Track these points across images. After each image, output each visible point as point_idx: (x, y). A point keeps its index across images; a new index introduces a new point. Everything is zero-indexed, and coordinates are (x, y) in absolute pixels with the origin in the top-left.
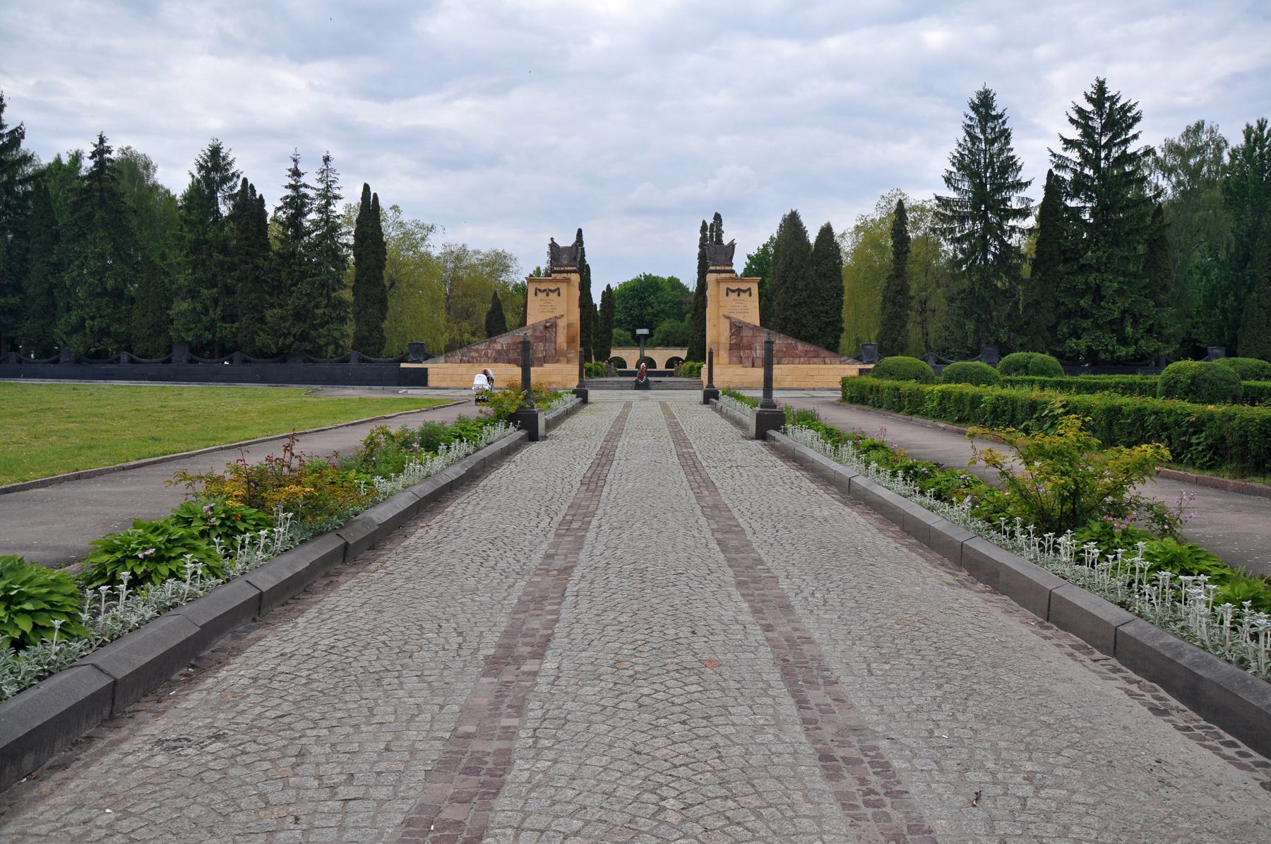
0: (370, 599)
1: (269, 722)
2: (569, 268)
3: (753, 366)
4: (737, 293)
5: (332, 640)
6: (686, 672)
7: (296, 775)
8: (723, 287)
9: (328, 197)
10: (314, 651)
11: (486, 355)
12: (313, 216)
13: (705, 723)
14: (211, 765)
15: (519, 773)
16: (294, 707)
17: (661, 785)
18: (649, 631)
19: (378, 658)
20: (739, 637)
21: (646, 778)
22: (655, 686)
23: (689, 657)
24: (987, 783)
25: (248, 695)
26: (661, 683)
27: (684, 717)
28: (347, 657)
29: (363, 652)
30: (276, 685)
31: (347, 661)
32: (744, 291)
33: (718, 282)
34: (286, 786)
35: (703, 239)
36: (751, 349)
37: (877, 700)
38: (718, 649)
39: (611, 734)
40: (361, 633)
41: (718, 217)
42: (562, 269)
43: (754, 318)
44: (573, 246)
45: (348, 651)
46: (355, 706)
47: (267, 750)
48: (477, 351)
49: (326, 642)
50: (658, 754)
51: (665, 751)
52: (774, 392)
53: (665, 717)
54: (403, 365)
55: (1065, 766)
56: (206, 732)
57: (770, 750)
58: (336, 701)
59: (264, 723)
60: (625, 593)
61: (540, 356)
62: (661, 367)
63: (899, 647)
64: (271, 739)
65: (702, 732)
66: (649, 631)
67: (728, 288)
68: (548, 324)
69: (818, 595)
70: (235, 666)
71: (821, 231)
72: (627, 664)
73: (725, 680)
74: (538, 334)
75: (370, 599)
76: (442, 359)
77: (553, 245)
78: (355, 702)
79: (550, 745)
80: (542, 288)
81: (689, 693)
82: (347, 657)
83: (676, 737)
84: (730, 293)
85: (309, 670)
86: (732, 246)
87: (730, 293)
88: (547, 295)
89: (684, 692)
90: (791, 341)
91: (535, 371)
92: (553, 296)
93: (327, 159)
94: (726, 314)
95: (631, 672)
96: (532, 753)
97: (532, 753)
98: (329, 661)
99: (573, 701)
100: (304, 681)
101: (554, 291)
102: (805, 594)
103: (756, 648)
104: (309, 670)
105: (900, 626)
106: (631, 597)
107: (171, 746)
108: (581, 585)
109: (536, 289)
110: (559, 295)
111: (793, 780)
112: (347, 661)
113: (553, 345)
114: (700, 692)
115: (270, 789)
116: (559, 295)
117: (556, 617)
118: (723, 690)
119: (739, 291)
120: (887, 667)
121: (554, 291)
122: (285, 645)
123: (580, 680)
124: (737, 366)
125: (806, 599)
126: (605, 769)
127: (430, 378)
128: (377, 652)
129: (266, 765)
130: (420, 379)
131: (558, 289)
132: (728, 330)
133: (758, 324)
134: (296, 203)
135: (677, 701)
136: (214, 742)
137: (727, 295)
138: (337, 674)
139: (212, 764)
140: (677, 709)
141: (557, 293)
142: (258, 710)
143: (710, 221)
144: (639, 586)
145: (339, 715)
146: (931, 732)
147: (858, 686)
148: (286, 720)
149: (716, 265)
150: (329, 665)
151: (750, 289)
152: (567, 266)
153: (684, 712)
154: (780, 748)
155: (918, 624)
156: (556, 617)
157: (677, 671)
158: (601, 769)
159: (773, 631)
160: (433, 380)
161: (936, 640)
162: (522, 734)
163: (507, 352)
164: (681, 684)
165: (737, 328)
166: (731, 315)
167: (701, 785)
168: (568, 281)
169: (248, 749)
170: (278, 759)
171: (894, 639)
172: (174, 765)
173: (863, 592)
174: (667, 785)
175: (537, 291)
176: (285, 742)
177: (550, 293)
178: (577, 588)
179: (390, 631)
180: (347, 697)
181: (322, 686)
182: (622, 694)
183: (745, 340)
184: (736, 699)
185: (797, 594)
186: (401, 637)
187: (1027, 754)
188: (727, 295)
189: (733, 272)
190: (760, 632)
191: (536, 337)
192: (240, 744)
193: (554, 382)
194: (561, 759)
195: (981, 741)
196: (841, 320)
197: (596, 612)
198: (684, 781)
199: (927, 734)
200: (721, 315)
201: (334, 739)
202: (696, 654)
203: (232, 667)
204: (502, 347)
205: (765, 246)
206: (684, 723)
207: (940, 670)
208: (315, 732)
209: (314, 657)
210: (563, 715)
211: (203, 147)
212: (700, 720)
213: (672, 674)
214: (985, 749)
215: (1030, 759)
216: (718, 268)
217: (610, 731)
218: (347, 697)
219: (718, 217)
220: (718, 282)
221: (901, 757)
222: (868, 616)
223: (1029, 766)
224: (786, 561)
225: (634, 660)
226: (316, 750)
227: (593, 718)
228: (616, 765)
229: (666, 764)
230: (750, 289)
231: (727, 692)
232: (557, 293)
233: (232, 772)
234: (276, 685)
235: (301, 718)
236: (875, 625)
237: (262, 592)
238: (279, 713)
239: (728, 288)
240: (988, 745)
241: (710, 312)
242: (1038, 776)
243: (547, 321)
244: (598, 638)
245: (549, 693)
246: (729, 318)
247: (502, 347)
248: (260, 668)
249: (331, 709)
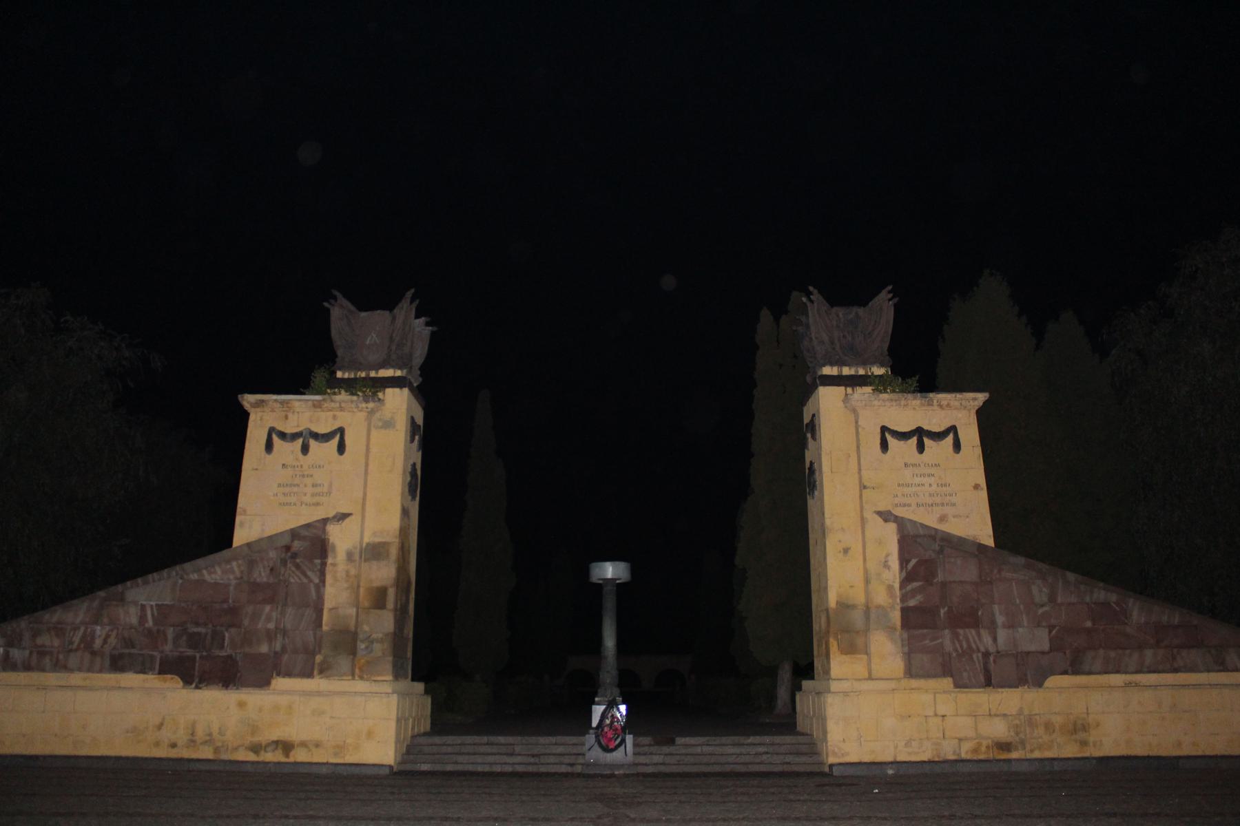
3: (988, 683)
4: (914, 441)
11: (87, 643)
32: (938, 436)
36: (976, 624)
48: (59, 630)
61: (264, 649)
67: (884, 429)
80: (289, 429)
88: (305, 449)
90: (1101, 594)
92: (323, 452)
101: (326, 438)
110: (341, 448)
113: (309, 613)
116: (341, 448)
119: (920, 435)
124: (932, 683)
133: (990, 542)
137: (884, 446)
149: (841, 363)
163: (154, 637)
166: (900, 512)
177: (313, 443)
188: (884, 446)
191: (255, 587)
193: (303, 744)
200: (869, 515)
204: (143, 618)
230: (953, 429)
239: (884, 429)
243: (294, 534)
247: (143, 618)
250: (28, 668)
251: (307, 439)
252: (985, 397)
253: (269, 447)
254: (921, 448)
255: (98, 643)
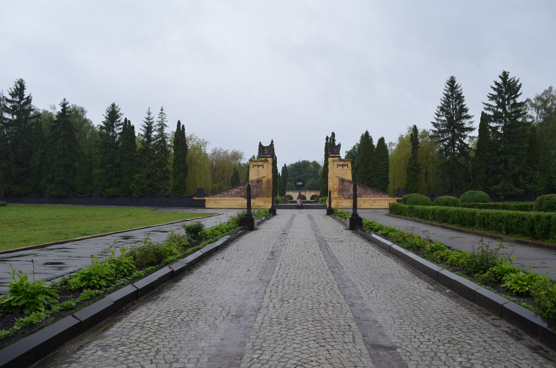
0: (183, 293)
1: (144, 339)
2: (268, 156)
4: (341, 166)
5: (168, 309)
6: (316, 322)
7: (155, 359)
8: (336, 164)
9: (162, 126)
10: (161, 313)
12: (155, 133)
13: (323, 341)
14: (121, 355)
15: (246, 359)
16: (153, 334)
17: (305, 363)
18: (301, 306)
19: (188, 316)
20: (339, 308)
21: (299, 360)
22: (303, 327)
23: (318, 316)
24: (442, 365)
25: (134, 329)
26: (306, 326)
27: (315, 338)
28: (175, 315)
29: (181, 313)
30: (145, 325)
31: (174, 316)
32: (345, 165)
33: (334, 161)
34: (152, 363)
35: (327, 144)
36: (348, 191)
37: (397, 334)
38: (330, 313)
39: (285, 344)
40: (180, 306)
41: (333, 134)
42: (265, 156)
43: (349, 176)
44: (269, 146)
45: (175, 313)
46: (179, 334)
47: (143, 350)
49: (166, 309)
50: (304, 352)
51: (306, 351)
52: (358, 210)
53: (307, 338)
54: (194, 198)
55: (476, 359)
56: (118, 343)
57: (350, 351)
58: (171, 332)
59: (141, 340)
60: (291, 291)
62: (308, 198)
63: (407, 313)
64: (144, 345)
65: (322, 344)
66: (301, 306)
68: (258, 180)
69: (374, 292)
70: (128, 318)
71: (379, 140)
72: (291, 318)
73: (333, 325)
74: (254, 184)
75: (183, 293)
76: (212, 196)
77: (260, 145)
78: (179, 332)
79: (259, 348)
81: (317, 329)
82: (175, 315)
83: (311, 346)
84: (338, 166)
85: (159, 320)
86: (339, 145)
87: (338, 166)
88: (258, 167)
89: (315, 329)
91: (252, 201)
92: (261, 168)
93: (162, 110)
94: (337, 175)
95: (293, 321)
96: (252, 351)
97: (252, 351)
98: (167, 317)
99: (269, 332)
100: (157, 324)
102: (368, 292)
103: (346, 313)
104: (159, 320)
105: (408, 305)
106: (293, 293)
107: (104, 349)
108: (272, 288)
109: (253, 165)
110: (263, 167)
111: (360, 363)
112: (174, 316)
114: (322, 329)
115: (145, 364)
116: (263, 167)
117: (262, 300)
118: (332, 329)
120: (402, 321)
121: (261, 166)
122: (149, 311)
123: (272, 324)
125: (368, 294)
126: (282, 357)
127: (206, 204)
128: (187, 313)
129: (143, 355)
130: (201, 205)
131: (263, 165)
132: (338, 182)
133: (351, 180)
134: (149, 129)
135: (312, 332)
136: (121, 346)
137: (337, 167)
138: (171, 322)
139: (121, 354)
140: (313, 335)
141: (262, 167)
142: (138, 335)
143: (330, 136)
144: (297, 288)
145: (172, 337)
146: (419, 346)
147: (389, 328)
148: (150, 338)
149: (333, 154)
150: (167, 318)
151: (347, 164)
152: (267, 155)
153: (314, 337)
154: (355, 351)
155: (416, 304)
156: (262, 300)
157: (313, 321)
158: (280, 357)
159: (354, 306)
160: (207, 205)
161: (423, 311)
162: (248, 344)
164: (314, 326)
165: (342, 181)
166: (340, 176)
167: (321, 364)
168: (267, 161)
169: (135, 349)
170: (148, 353)
171: (405, 311)
172: (106, 355)
173: (393, 291)
174: (307, 363)
175: (254, 166)
176: (150, 347)
178: (271, 289)
179: (192, 305)
180: (175, 330)
181: (164, 326)
182: (290, 329)
183: (346, 187)
184: (337, 332)
185: (365, 292)
186: (197, 308)
187: (459, 355)
188: (337, 167)
189: (340, 157)
190: (348, 307)
192: (133, 347)
194: (263, 354)
195: (440, 350)
196: (388, 178)
197: (279, 299)
198: (314, 362)
199: (417, 347)
201: (170, 346)
202: (321, 315)
203: (127, 319)
205: (354, 146)
206: (315, 340)
207: (425, 322)
208: (163, 343)
209: (160, 315)
210: (264, 337)
211: (109, 105)
212: (322, 340)
213: (310, 322)
214: (441, 353)
215: (460, 357)
216: (333, 155)
217: (284, 343)
218: (175, 330)
219: (333, 134)
220: (334, 161)
221: (405, 355)
222: (395, 301)
223: (460, 359)
224: (361, 280)
225: (295, 317)
226: (162, 349)
227: (278, 338)
228: (287, 356)
229: (307, 355)
230: (347, 164)
231: (333, 329)
232: (262, 167)
233: (129, 357)
234: (145, 325)
235: (156, 338)
236: (397, 305)
237: (138, 289)
238: (147, 336)
240: (443, 351)
241: (330, 174)
242: (463, 363)
244: (279, 308)
245: (259, 329)
246: (338, 177)
248: (139, 319)
249: (169, 335)
250: (223, 197)
251: (259, 166)
252: (391, 144)
253: (253, 167)
254: (343, 167)
255: (232, 194)
